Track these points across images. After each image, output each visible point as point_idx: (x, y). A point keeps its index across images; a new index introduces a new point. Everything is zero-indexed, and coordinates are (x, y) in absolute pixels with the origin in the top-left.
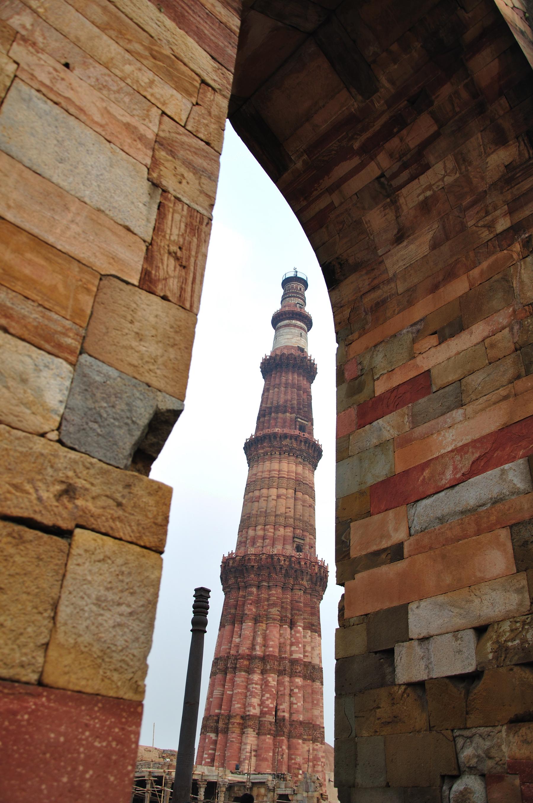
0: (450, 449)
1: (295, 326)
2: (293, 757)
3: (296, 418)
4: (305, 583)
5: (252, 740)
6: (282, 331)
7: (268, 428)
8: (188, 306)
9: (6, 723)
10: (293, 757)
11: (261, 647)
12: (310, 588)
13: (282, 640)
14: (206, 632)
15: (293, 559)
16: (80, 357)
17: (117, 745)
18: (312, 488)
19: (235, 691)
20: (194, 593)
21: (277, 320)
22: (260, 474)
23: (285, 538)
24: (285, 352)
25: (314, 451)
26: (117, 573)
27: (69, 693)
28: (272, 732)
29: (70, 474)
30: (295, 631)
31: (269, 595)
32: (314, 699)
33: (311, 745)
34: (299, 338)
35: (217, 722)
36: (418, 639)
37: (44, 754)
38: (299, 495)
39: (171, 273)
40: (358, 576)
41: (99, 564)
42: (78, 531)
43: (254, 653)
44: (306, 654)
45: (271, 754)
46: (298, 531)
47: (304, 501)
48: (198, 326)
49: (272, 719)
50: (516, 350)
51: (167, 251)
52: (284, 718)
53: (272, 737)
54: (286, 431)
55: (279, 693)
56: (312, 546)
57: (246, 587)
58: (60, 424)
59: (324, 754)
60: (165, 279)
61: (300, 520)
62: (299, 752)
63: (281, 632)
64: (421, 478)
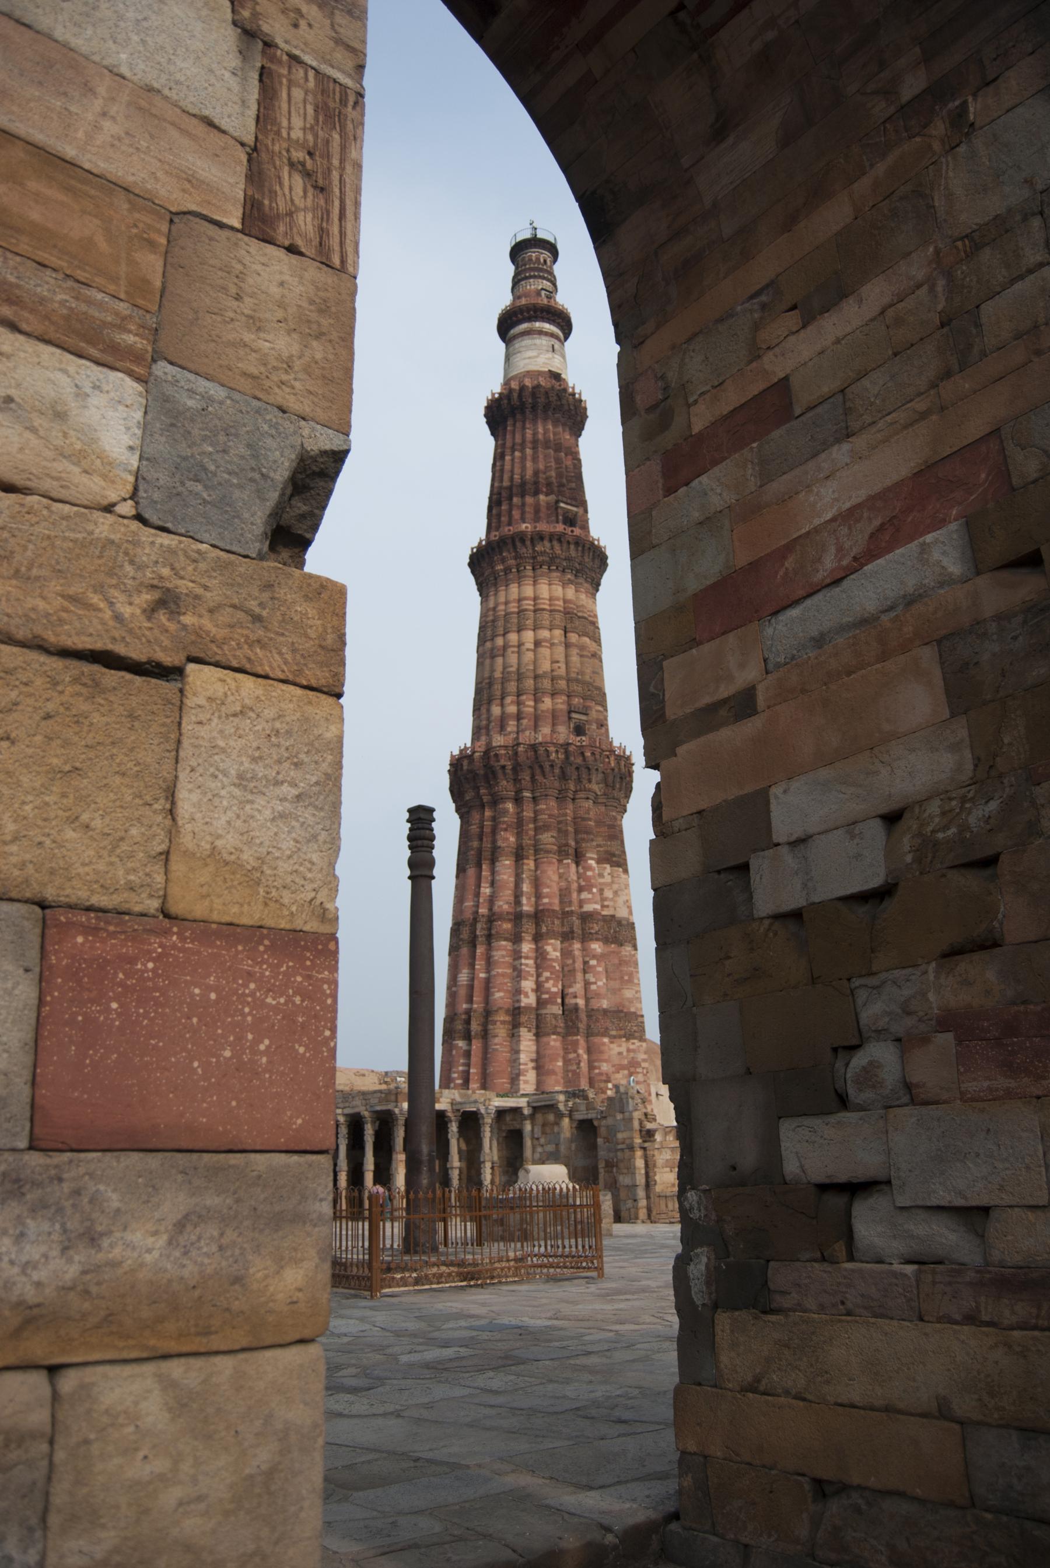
0: (829, 516)
1: (541, 333)
2: (596, 1064)
3: (557, 502)
4: (595, 787)
5: (527, 1046)
6: (518, 344)
7: (510, 524)
8: (336, 261)
9: (121, 976)
10: (596, 1064)
11: (529, 899)
12: (605, 794)
13: (563, 884)
14: (433, 878)
15: (571, 748)
16: (154, 367)
17: (303, 1001)
18: (594, 624)
19: (493, 973)
20: (407, 815)
21: (508, 325)
22: (502, 607)
23: (554, 714)
24: (528, 382)
25: (593, 560)
26: (268, 732)
27: (214, 926)
28: (559, 1030)
29: (166, 571)
30: (583, 868)
31: (535, 812)
32: (623, 972)
33: (624, 1045)
34: (550, 355)
35: (468, 1022)
36: (789, 844)
37: (189, 1018)
38: (573, 637)
39: (299, 202)
40: (681, 750)
41: (236, 720)
42: (191, 667)
43: (518, 909)
44: (606, 903)
45: (560, 1064)
46: (576, 701)
47: (582, 648)
48: (359, 298)
49: (557, 1010)
50: (943, 325)
51: (285, 161)
52: (576, 1008)
53: (560, 1038)
55: (566, 969)
56: (603, 724)
57: (495, 802)
58: (136, 489)
59: (645, 1057)
60: (290, 214)
61: (577, 681)
62: (606, 1057)
63: (561, 871)
64: (781, 573)
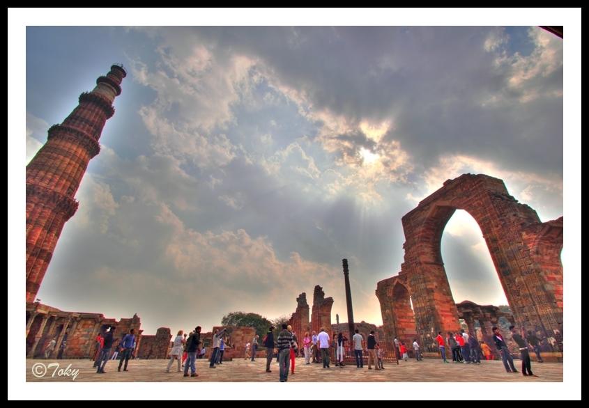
21: (101, 81)
38: (81, 169)
54: (90, 135)
